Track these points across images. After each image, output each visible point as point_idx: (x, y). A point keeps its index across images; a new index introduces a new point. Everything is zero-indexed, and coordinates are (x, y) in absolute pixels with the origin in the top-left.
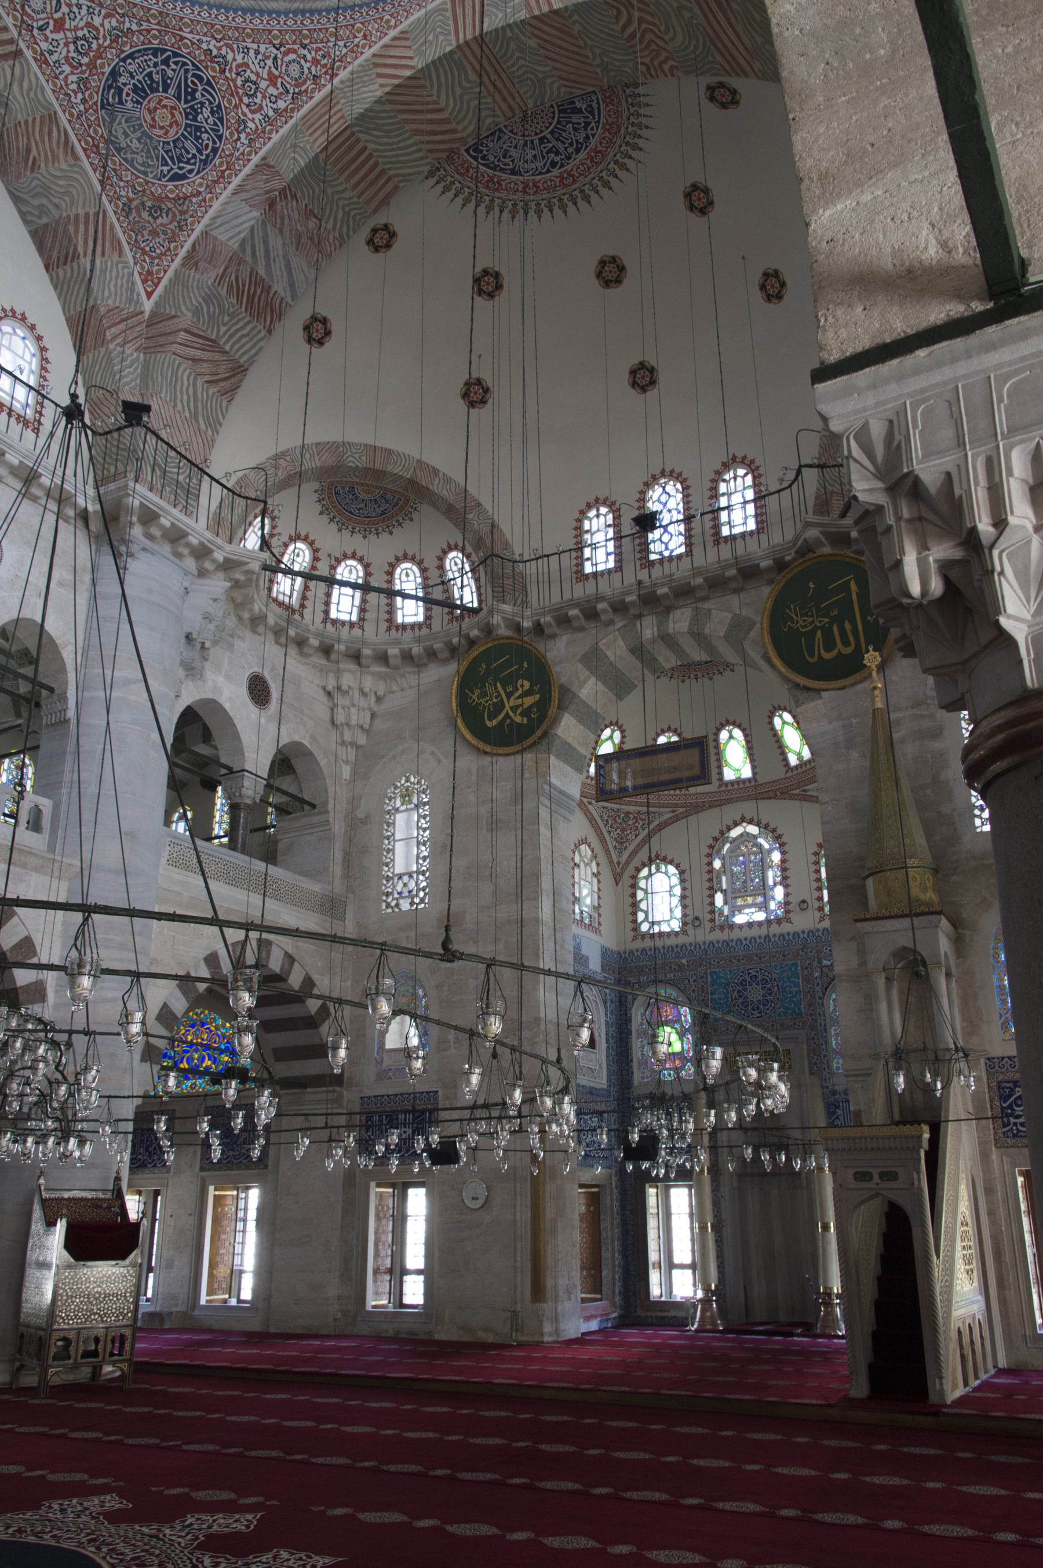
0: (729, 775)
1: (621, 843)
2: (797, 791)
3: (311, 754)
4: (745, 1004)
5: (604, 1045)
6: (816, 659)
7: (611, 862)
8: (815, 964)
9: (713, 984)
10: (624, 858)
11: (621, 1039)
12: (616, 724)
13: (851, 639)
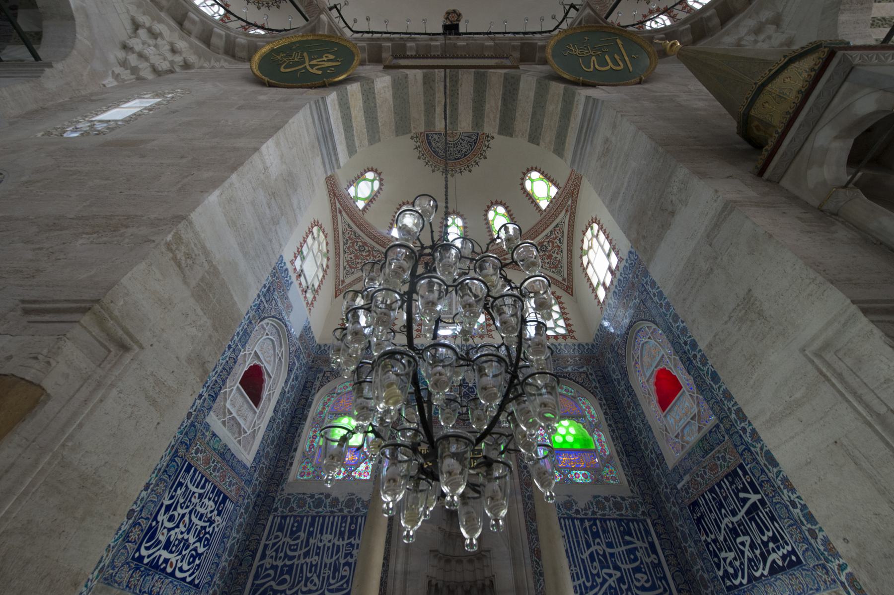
1: (351, 267)
3: (72, 18)
5: (269, 413)
6: (591, 70)
7: (337, 277)
10: (348, 281)
11: (291, 425)
12: (380, 174)
13: (620, 63)
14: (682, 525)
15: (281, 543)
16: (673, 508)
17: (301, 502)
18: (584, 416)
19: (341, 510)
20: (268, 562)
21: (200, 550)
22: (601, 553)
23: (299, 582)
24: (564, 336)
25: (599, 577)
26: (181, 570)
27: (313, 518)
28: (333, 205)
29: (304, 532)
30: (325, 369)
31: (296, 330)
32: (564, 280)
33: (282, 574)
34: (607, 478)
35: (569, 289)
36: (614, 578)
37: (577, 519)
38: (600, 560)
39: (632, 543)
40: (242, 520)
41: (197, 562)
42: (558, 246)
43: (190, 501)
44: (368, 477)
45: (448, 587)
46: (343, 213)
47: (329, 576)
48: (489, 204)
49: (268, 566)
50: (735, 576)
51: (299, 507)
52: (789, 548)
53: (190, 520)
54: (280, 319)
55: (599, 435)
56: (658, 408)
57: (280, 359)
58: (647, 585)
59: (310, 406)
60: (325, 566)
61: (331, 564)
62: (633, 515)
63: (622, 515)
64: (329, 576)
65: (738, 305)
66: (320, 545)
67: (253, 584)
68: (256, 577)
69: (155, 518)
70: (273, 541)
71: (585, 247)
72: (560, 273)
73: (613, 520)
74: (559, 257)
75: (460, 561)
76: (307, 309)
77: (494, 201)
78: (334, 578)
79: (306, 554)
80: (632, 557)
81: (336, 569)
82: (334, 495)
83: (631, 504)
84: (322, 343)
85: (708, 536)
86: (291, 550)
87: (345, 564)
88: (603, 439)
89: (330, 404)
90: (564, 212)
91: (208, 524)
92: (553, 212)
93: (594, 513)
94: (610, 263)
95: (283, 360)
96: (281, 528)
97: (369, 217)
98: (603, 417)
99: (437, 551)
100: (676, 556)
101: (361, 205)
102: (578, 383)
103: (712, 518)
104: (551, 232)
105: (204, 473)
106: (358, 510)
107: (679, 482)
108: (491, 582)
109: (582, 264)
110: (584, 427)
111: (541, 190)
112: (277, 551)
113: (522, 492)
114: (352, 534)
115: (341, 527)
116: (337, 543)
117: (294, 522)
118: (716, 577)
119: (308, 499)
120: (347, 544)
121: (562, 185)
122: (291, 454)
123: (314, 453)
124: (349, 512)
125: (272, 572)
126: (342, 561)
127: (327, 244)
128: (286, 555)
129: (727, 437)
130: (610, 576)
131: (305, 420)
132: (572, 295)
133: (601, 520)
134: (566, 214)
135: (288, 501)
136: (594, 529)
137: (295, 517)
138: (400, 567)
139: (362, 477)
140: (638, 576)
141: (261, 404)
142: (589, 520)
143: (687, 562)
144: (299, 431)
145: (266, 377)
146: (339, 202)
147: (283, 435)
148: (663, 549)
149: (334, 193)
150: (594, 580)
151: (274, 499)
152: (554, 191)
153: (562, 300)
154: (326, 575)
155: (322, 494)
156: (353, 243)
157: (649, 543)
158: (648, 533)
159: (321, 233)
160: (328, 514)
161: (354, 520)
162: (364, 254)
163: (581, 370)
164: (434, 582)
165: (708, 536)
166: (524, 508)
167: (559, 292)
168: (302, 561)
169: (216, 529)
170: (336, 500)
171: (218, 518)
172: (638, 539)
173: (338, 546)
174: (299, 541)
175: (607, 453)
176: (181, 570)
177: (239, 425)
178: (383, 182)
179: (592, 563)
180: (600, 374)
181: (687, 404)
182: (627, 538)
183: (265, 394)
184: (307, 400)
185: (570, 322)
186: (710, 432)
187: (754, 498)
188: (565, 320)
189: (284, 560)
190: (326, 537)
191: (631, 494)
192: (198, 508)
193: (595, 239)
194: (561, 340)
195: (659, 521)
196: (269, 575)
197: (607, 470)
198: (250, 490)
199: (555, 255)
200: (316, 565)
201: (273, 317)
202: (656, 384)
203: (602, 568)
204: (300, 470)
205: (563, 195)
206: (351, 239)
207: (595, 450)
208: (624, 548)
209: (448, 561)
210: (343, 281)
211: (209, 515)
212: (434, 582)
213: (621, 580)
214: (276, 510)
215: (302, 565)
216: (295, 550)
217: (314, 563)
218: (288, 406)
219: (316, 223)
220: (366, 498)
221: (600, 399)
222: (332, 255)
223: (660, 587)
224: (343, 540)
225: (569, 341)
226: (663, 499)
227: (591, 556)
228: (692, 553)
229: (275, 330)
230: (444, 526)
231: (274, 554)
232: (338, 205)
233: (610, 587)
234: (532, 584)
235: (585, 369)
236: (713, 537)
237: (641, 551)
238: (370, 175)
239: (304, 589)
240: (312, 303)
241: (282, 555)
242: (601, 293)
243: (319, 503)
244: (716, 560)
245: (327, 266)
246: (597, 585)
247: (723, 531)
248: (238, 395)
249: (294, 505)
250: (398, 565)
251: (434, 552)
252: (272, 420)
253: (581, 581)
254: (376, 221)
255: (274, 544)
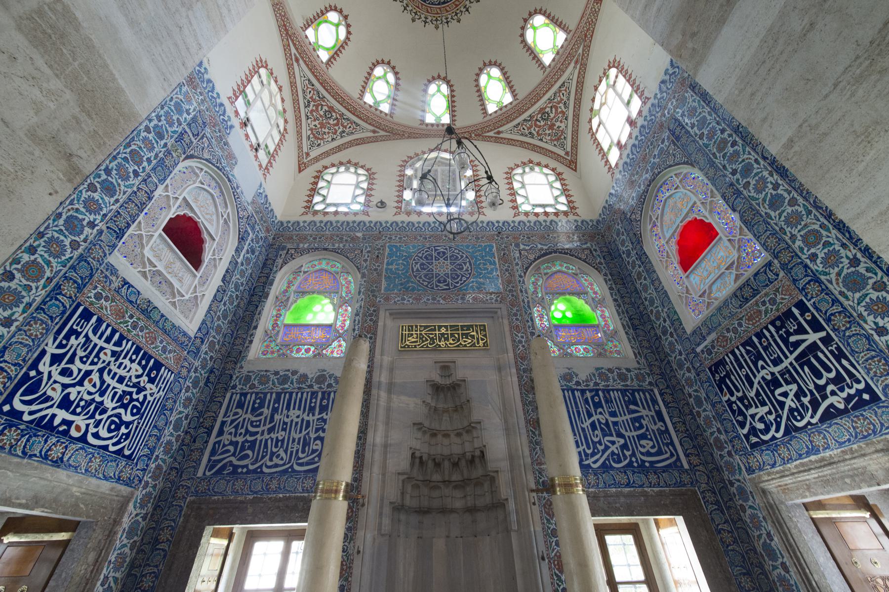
0: (430, 119)
2: (491, 134)
4: (429, 276)
5: (216, 281)
7: (300, 147)
8: (512, 247)
9: (390, 255)
10: (314, 154)
14: (697, 389)
15: (241, 419)
16: (687, 374)
17: (264, 378)
18: (587, 293)
19: (311, 386)
20: (226, 438)
21: (128, 418)
22: (604, 422)
23: (263, 457)
24: (566, 213)
25: (601, 444)
26: (96, 436)
27: (278, 395)
28: (286, 48)
29: (268, 408)
30: (289, 246)
31: (248, 195)
32: (567, 153)
33: (243, 448)
34: (611, 352)
35: (573, 164)
36: (617, 445)
37: (578, 390)
38: (602, 429)
39: (638, 412)
40: (189, 394)
41: (123, 430)
42: (562, 112)
43: (97, 356)
44: (342, 355)
45: (434, 459)
46: (301, 62)
47: (297, 451)
48: (481, 65)
49: (227, 443)
50: (767, 430)
51: (261, 383)
52: (861, 386)
53: (103, 382)
54: (218, 168)
55: (603, 311)
56: (680, 271)
57: (226, 222)
58: (653, 451)
59: (271, 284)
60: (294, 440)
61: (300, 439)
62: (639, 386)
63: (627, 385)
64: (297, 451)
65: (858, 57)
66: (286, 420)
67: (209, 460)
68: (213, 452)
69: (34, 366)
70: (231, 418)
71: (596, 106)
72: (562, 146)
73: (617, 390)
74: (563, 125)
75: (446, 436)
76: (261, 173)
77: (487, 62)
78: (303, 452)
79: (271, 430)
80: (637, 425)
81: (306, 443)
82: (302, 371)
83: (637, 375)
84: (284, 220)
85: (732, 394)
86: (252, 426)
87: (315, 439)
88: (607, 314)
89: (297, 283)
90: (572, 64)
91: (135, 390)
92: (558, 66)
93: (596, 384)
94: (629, 112)
95: (231, 225)
96: (240, 405)
97: (336, 74)
98: (608, 292)
99: (420, 424)
100: (684, 423)
101: (324, 56)
102: (580, 259)
103: (742, 373)
104: (555, 94)
105: (116, 327)
106: (330, 386)
107: (699, 345)
108: (482, 452)
109: (591, 129)
110: (586, 303)
111: (545, 38)
112: (236, 427)
113: (517, 366)
114: (324, 409)
115: (311, 402)
116: (306, 418)
117: (256, 399)
118: (738, 436)
119: (272, 376)
120: (318, 419)
121: (572, 27)
122: (251, 332)
123: (278, 332)
124: (320, 388)
125: (231, 448)
126: (313, 436)
127: (283, 100)
128: (247, 431)
129: (782, 274)
130: (613, 443)
131: (266, 297)
132: (575, 170)
133: (603, 391)
134: (575, 67)
135: (248, 378)
136: (596, 399)
137: (257, 394)
138: (379, 440)
139: (335, 355)
140: (643, 442)
141: (203, 268)
142: (591, 391)
143: (698, 427)
144: (259, 309)
145: (205, 236)
146: (295, 45)
147: (241, 312)
148: (670, 417)
149: (286, 30)
150: (595, 447)
151: (231, 377)
152: (561, 37)
153: (564, 176)
154: (295, 450)
155: (289, 370)
156: (317, 106)
157: (655, 411)
158: (655, 402)
159: (272, 82)
160: (296, 390)
161: (326, 395)
162: (331, 122)
163: (585, 246)
164: (418, 454)
165: (732, 394)
166: (519, 381)
167: (561, 168)
168: (266, 436)
169: (149, 398)
170: (304, 377)
171: (149, 386)
172: (644, 408)
173: (308, 422)
174: (263, 417)
175: (611, 328)
176: (96, 436)
177: (171, 285)
178: (351, 29)
179: (593, 431)
180: (605, 250)
181: (722, 254)
182: (632, 407)
183: (207, 256)
184: (268, 278)
185: (572, 198)
186: (756, 274)
187: (813, 337)
188: (567, 196)
189: (245, 436)
190: (294, 413)
191: (638, 366)
192: (112, 367)
193: (611, 90)
194: (561, 216)
195: (668, 391)
196: (228, 451)
197: (610, 344)
198: (197, 363)
199: (558, 124)
200: (283, 441)
201: (206, 160)
202: (679, 243)
203: (604, 436)
204: (263, 349)
205: (573, 41)
206: (314, 101)
207: (598, 326)
208: (628, 417)
209: (434, 435)
210: (308, 154)
211: (134, 380)
212: (418, 454)
213: (624, 447)
214: (234, 387)
215: (266, 441)
216: (258, 426)
217: (280, 438)
218: (243, 280)
219: (261, 64)
220: (338, 374)
221: (605, 275)
222: (290, 115)
223: (666, 452)
224: (313, 415)
225: (571, 217)
226: (675, 367)
227: (593, 425)
228: (707, 417)
229: (213, 184)
230: (429, 399)
231: (233, 430)
232: (293, 51)
233: (613, 453)
234: (527, 452)
235: (589, 245)
236: (740, 394)
237: (647, 419)
238: (333, 16)
239: (269, 464)
240: (267, 168)
241: (243, 431)
242: (614, 156)
243: (284, 380)
244: (740, 418)
245: (285, 129)
246: (599, 452)
247: (756, 385)
248: (158, 241)
249: (256, 383)
250: (377, 437)
251: (419, 426)
252: (221, 291)
253: (581, 449)
254: (344, 77)
255: (232, 422)
